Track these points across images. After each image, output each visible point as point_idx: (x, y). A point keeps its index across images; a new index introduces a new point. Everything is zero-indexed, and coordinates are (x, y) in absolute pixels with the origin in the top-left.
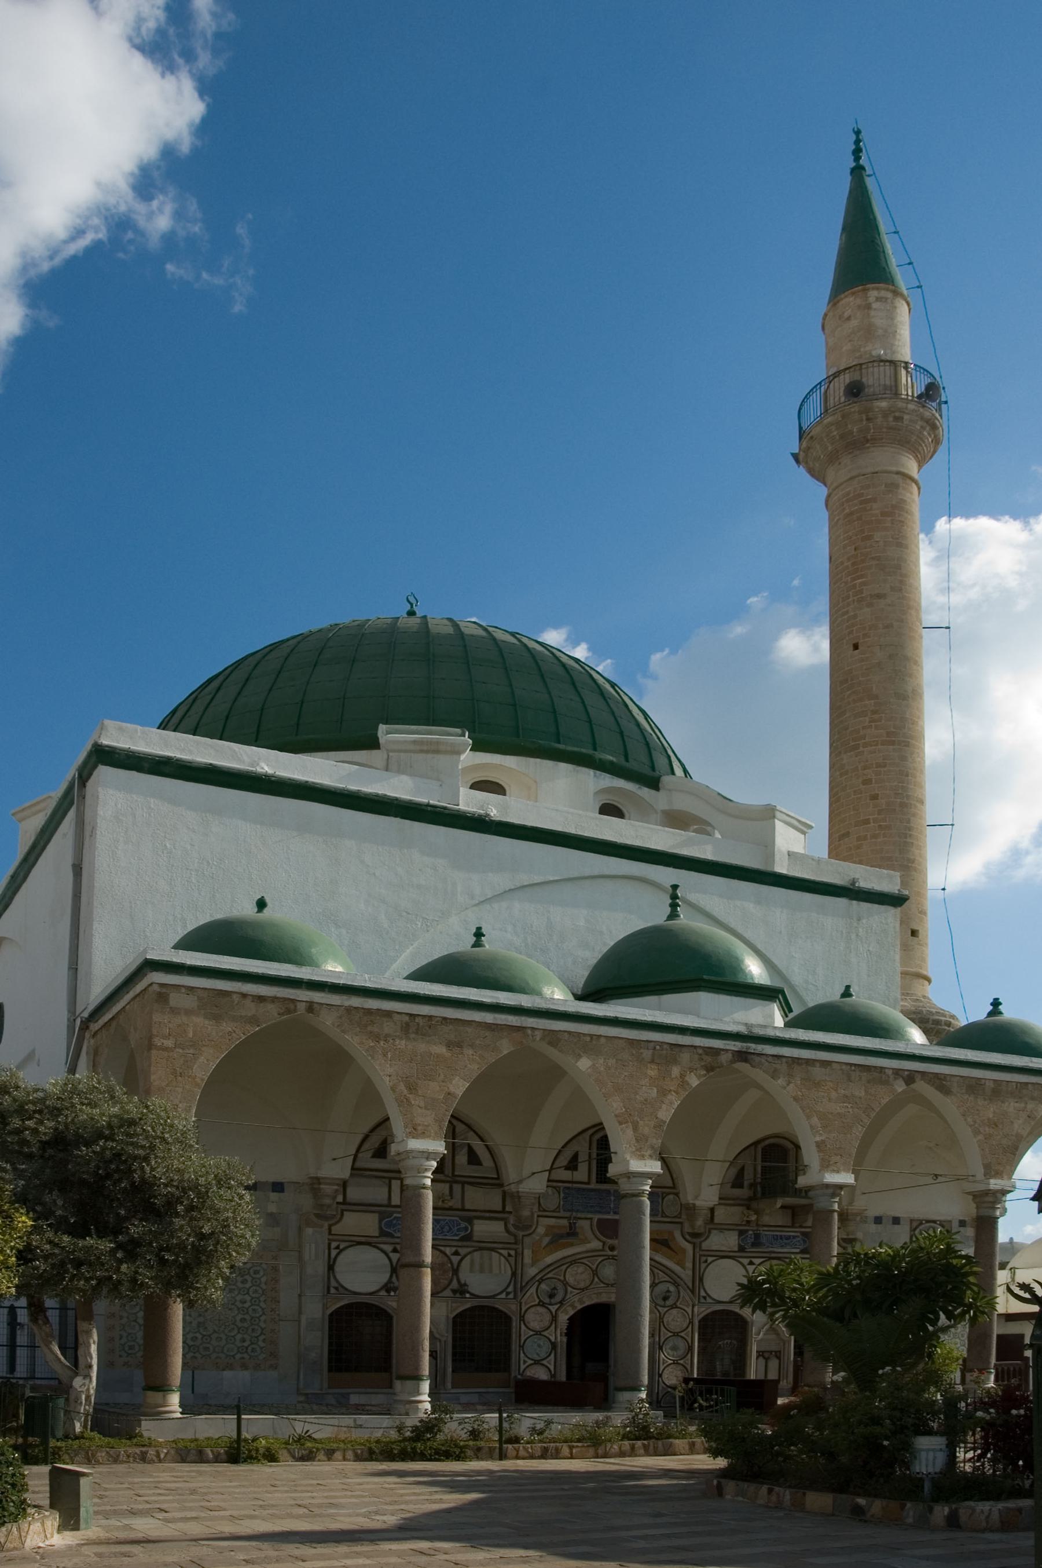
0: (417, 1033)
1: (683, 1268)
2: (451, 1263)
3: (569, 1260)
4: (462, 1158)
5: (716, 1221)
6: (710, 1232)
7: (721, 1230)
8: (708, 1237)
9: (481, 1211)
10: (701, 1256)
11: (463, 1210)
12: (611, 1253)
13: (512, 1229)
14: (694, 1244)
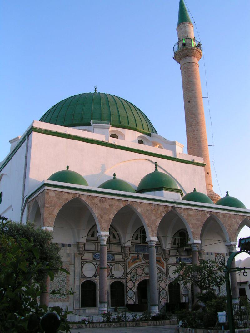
0: (102, 202)
1: (164, 268)
2: (110, 268)
3: (137, 266)
4: (112, 237)
5: (171, 254)
7: (172, 257)
9: (117, 252)
11: (112, 252)
14: (166, 261)
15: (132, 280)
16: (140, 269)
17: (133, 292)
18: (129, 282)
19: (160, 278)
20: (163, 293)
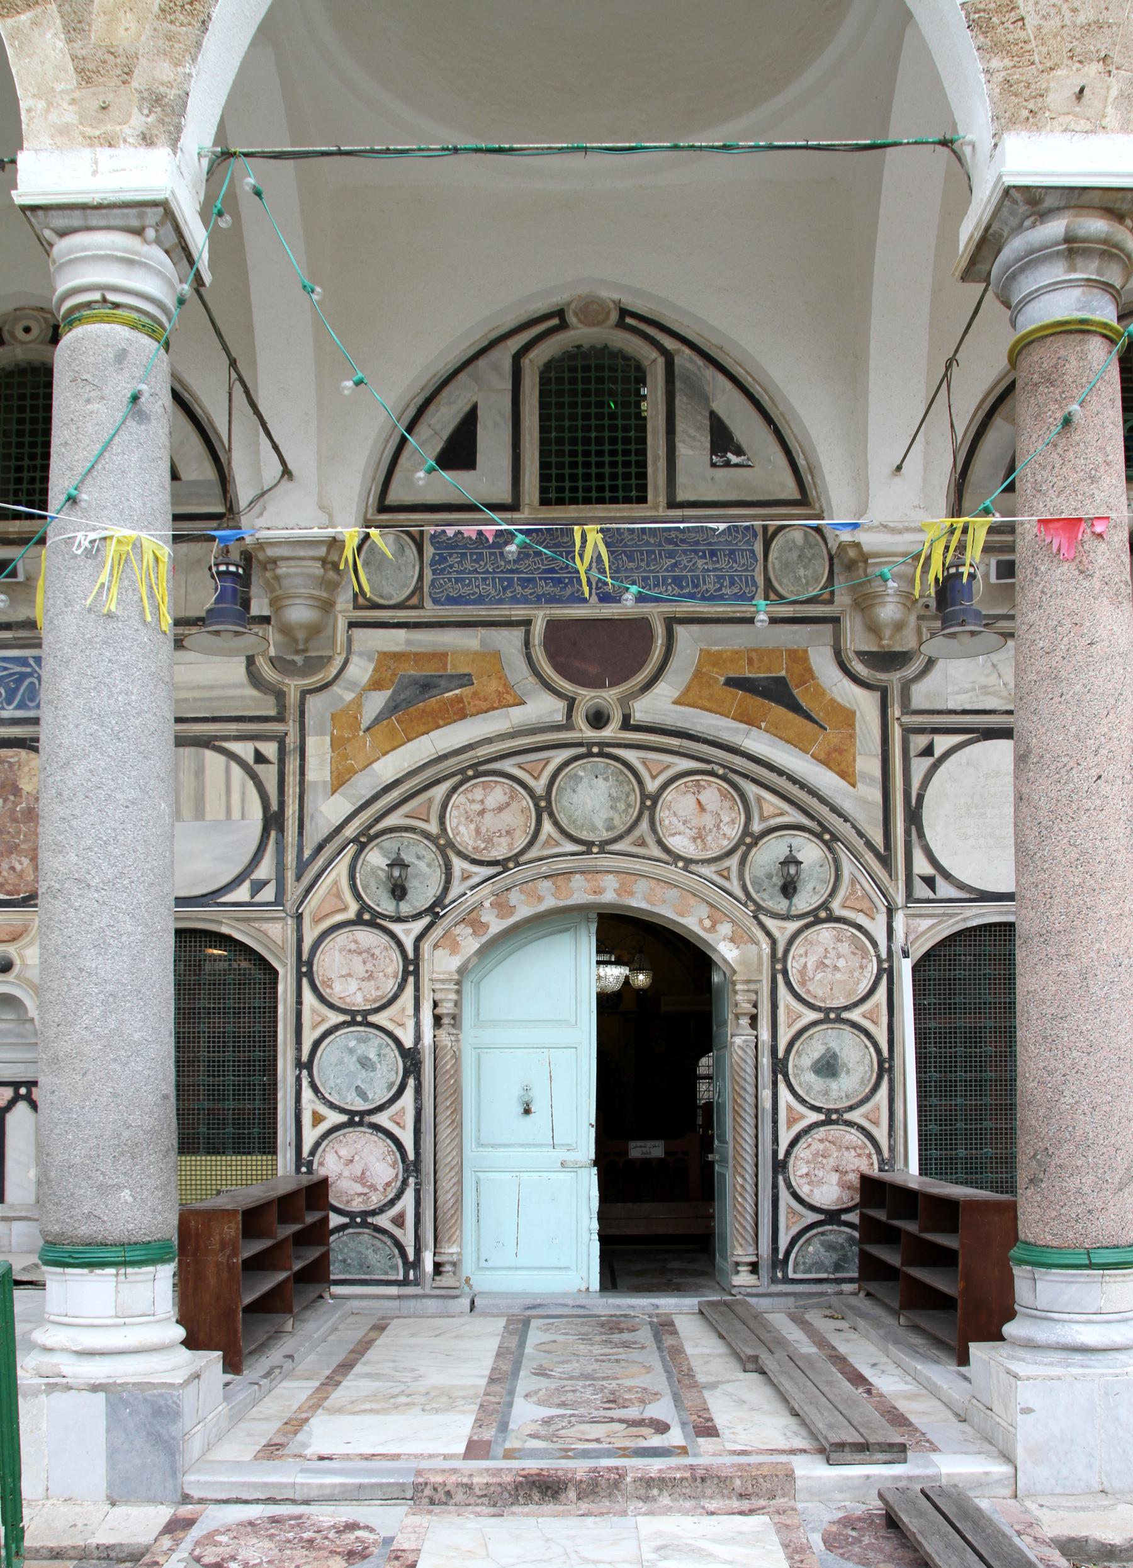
1: (847, 775)
10: (908, 731)
12: (590, 734)
13: (268, 673)
15: (376, 915)
16: (498, 794)
17: (393, 1053)
18: (342, 938)
19: (789, 889)
20: (828, 1067)
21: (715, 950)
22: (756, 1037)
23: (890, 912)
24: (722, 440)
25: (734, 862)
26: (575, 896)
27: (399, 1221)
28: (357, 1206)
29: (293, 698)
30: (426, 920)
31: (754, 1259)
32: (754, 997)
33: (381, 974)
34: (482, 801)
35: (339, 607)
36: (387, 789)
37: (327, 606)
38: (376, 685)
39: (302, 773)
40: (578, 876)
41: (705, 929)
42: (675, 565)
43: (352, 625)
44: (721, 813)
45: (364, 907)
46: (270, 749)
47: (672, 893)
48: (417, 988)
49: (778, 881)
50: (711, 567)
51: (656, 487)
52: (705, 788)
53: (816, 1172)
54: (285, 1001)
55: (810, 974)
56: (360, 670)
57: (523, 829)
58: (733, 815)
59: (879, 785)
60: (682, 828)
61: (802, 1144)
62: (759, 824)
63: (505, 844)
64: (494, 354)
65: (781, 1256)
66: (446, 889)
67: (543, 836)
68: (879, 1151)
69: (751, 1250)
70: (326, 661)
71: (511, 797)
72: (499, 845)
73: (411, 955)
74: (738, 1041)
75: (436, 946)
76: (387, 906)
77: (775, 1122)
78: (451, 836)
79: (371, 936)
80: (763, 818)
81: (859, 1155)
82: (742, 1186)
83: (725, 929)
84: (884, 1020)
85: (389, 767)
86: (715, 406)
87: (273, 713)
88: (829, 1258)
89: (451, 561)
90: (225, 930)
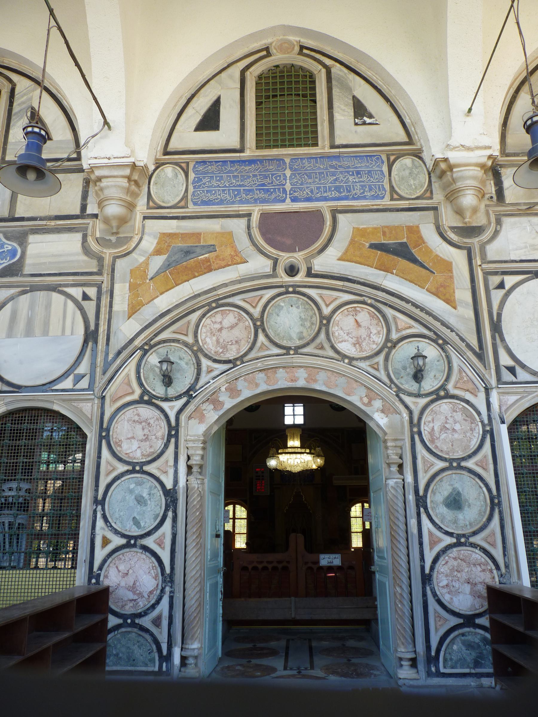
1: (450, 301)
6: (499, 222)
8: (496, 233)
10: (487, 274)
17: (159, 493)
18: (129, 412)
20: (455, 502)
21: (372, 419)
22: (403, 480)
23: (487, 390)
24: (360, 110)
25: (381, 359)
26: (279, 383)
27: (157, 622)
28: (129, 610)
29: (107, 261)
30: (184, 400)
31: (412, 656)
32: (399, 451)
33: (154, 437)
34: (221, 323)
35: (138, 208)
36: (162, 315)
37: (131, 207)
38: (158, 252)
39: (111, 306)
40: (281, 370)
41: (364, 404)
42: (336, 180)
43: (145, 218)
44: (371, 327)
45: (145, 392)
46: (92, 292)
47: (342, 380)
48: (177, 447)
49: (411, 371)
50: (357, 180)
51: (323, 137)
52: (360, 312)
53: (454, 584)
54: (90, 455)
55: (437, 434)
56: (149, 244)
57: (246, 339)
58: (379, 329)
59: (472, 308)
60: (347, 338)
61: (441, 561)
62: (396, 334)
63: (234, 349)
64: (230, 71)
65: (433, 654)
66: (197, 379)
67: (258, 344)
68: (498, 567)
69: (410, 648)
70: (129, 239)
71: (239, 320)
72: (231, 350)
73: (173, 423)
74: (391, 482)
75: (190, 418)
76: (159, 390)
77: (421, 544)
78: (201, 344)
79: (148, 410)
80: (398, 330)
81: (484, 570)
82: (401, 594)
83: (378, 404)
84: (491, 467)
85: (164, 302)
86: (356, 94)
87: (95, 270)
88: (470, 656)
89: (204, 181)
90: (56, 408)
